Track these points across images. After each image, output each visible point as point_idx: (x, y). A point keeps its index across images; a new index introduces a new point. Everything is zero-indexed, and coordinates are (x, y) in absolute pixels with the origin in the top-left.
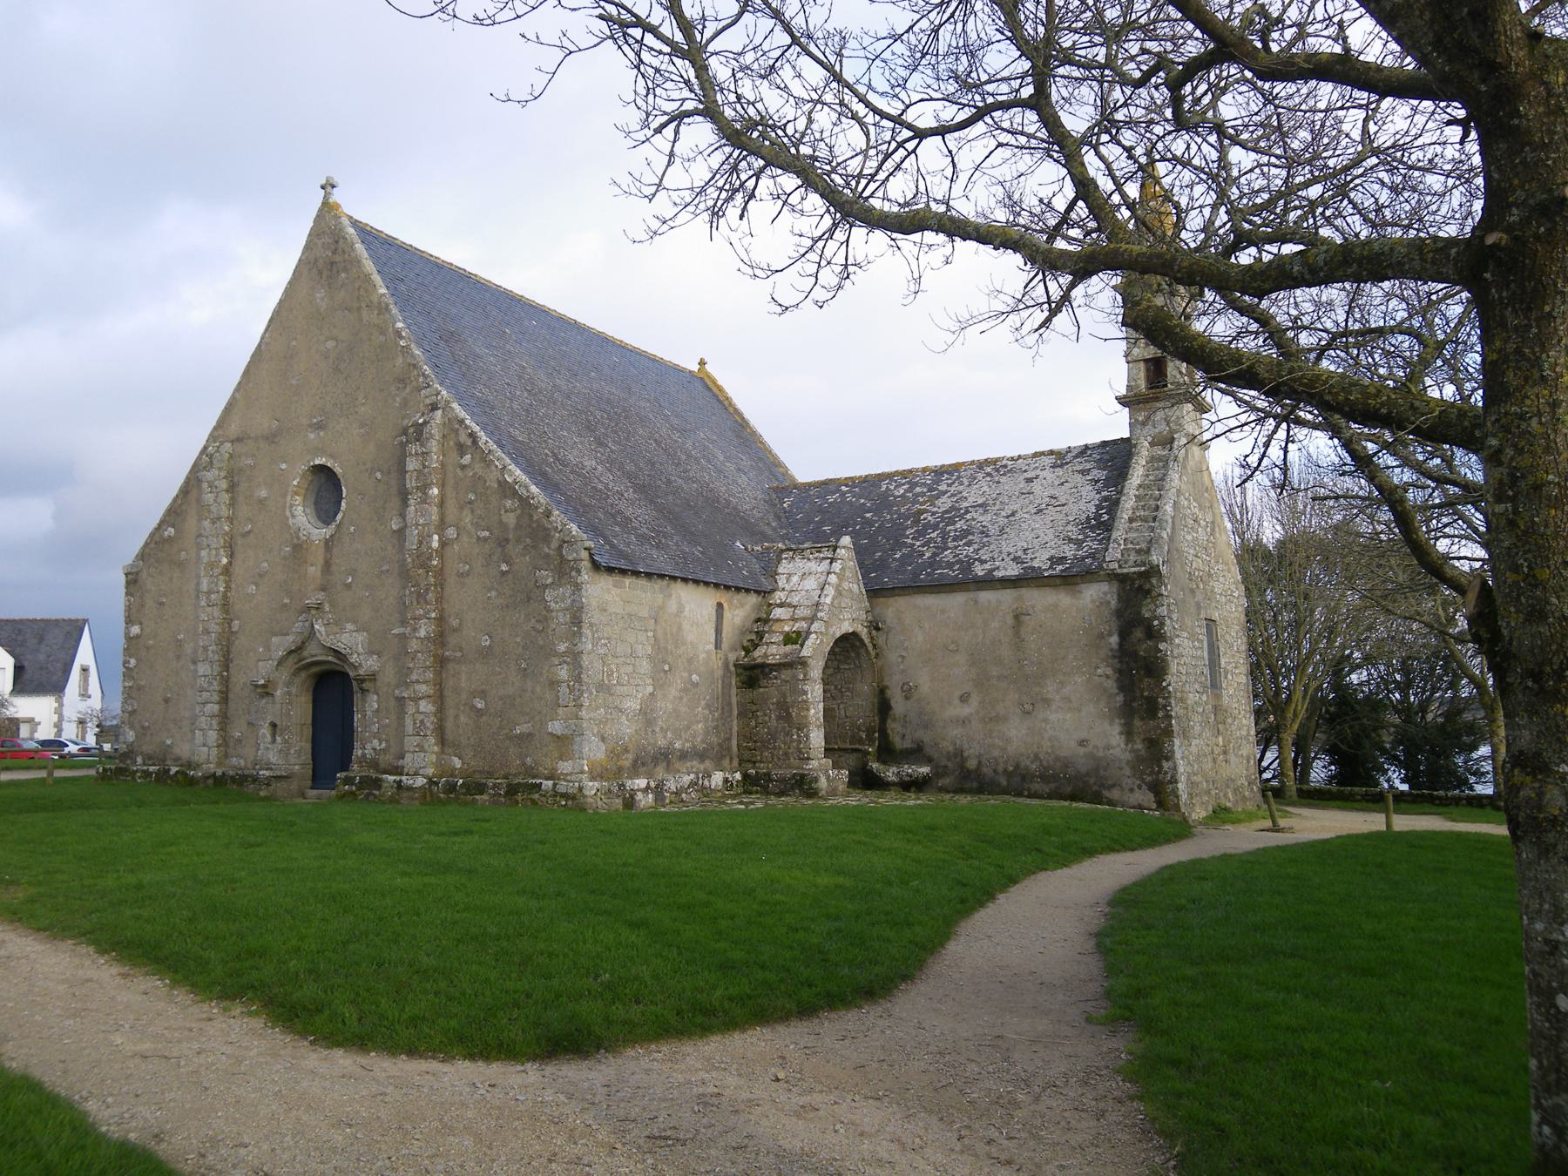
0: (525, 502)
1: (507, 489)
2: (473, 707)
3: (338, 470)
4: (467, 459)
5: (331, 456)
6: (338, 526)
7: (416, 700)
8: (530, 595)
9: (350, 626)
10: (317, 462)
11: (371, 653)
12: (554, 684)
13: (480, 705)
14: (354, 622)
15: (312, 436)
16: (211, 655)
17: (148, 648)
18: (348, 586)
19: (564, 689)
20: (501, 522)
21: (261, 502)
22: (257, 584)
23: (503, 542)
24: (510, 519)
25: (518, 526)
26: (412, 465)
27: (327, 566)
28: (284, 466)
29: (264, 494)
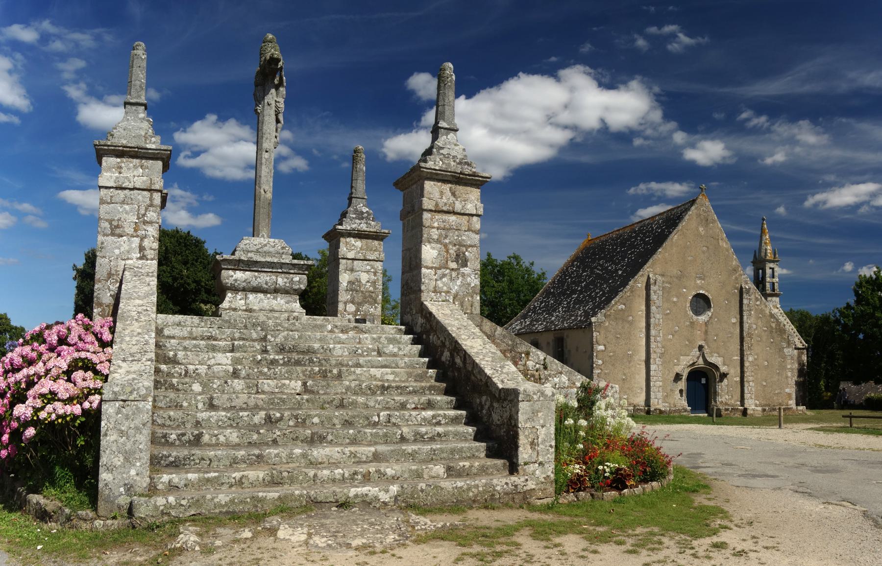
0: (778, 322)
1: (772, 315)
2: (762, 385)
3: (710, 297)
4: (758, 303)
5: (707, 291)
6: (711, 318)
7: (748, 382)
8: (781, 350)
9: (716, 355)
10: (701, 292)
11: (724, 364)
12: (787, 377)
13: (765, 384)
14: (718, 353)
15: (698, 282)
16: (657, 362)
17: (610, 357)
18: (715, 340)
19: (790, 379)
20: (771, 326)
21: (674, 302)
22: (673, 335)
23: (771, 332)
24: (774, 325)
25: (776, 329)
26: (745, 301)
27: (706, 332)
28: (685, 290)
29: (675, 299)
